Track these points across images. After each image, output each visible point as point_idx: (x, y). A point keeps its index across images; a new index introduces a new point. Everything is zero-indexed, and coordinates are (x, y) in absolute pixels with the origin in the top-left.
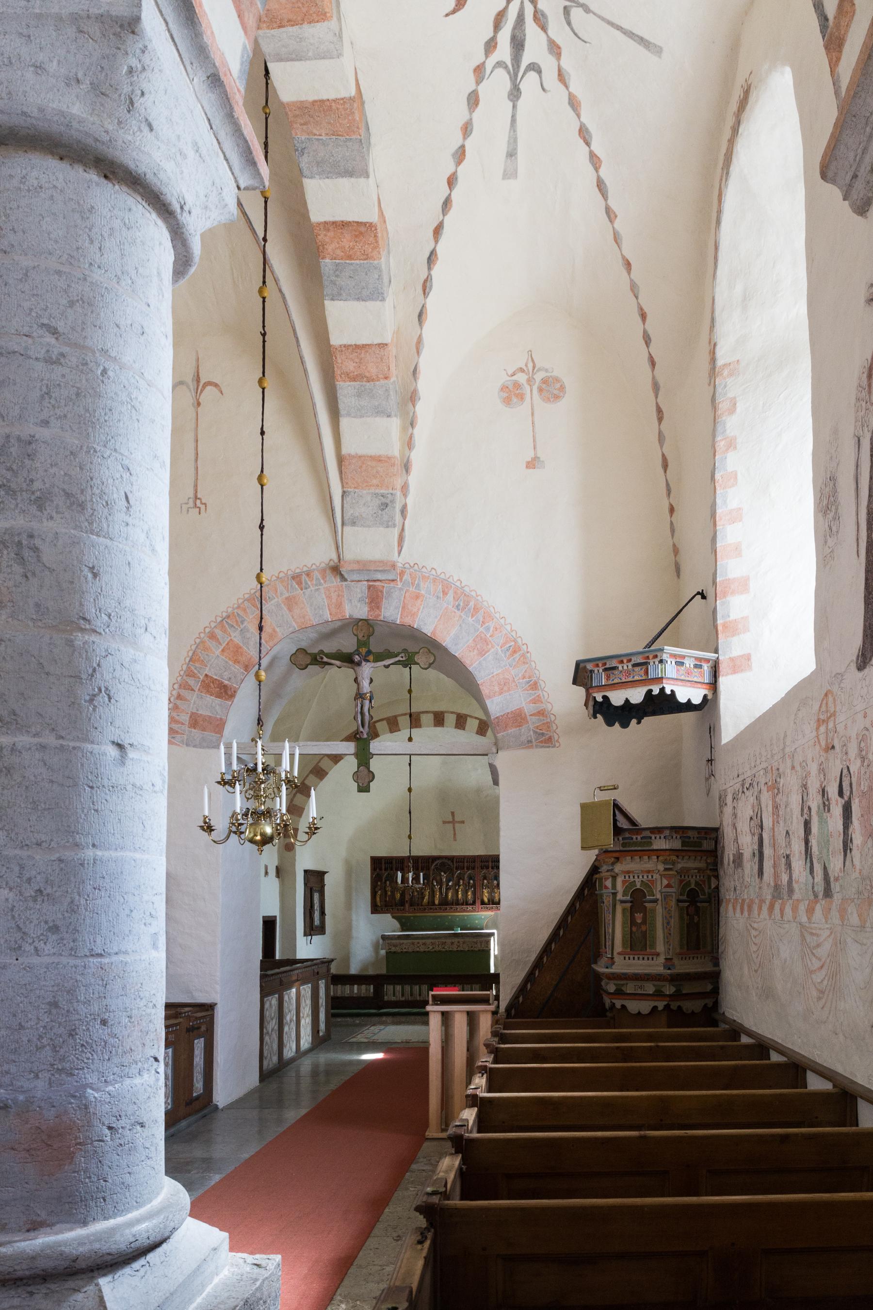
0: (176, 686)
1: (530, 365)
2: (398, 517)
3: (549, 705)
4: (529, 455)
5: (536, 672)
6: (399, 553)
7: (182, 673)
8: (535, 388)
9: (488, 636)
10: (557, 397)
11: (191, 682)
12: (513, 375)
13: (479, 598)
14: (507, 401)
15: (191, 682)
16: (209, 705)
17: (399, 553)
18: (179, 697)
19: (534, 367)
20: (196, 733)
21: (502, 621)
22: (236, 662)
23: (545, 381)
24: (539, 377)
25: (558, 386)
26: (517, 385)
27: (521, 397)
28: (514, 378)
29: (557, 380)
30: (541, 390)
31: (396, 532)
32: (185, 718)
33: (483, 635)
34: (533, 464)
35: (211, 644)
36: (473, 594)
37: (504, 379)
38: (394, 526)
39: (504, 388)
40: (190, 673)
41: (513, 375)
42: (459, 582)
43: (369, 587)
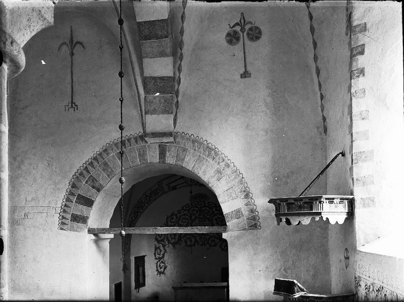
0: (64, 200)
1: (242, 21)
2: (174, 107)
3: (254, 206)
4: (242, 71)
5: (248, 189)
6: (175, 127)
7: (67, 193)
8: (245, 34)
9: (222, 170)
10: (258, 38)
11: (71, 198)
12: (234, 26)
13: (217, 149)
14: (230, 42)
15: (71, 198)
16: (80, 210)
17: (175, 127)
18: (66, 206)
19: (244, 22)
20: (75, 224)
21: (229, 162)
22: (93, 187)
23: (251, 29)
24: (247, 27)
25: (257, 31)
26: (235, 32)
27: (238, 39)
28: (234, 29)
29: (257, 28)
30: (248, 34)
31: (172, 116)
32: (69, 216)
33: (219, 170)
34: (245, 75)
35: (81, 178)
36: (213, 147)
37: (227, 30)
38: (172, 113)
39: (228, 35)
40: (72, 194)
41: (234, 26)
42: (206, 141)
43: (159, 145)
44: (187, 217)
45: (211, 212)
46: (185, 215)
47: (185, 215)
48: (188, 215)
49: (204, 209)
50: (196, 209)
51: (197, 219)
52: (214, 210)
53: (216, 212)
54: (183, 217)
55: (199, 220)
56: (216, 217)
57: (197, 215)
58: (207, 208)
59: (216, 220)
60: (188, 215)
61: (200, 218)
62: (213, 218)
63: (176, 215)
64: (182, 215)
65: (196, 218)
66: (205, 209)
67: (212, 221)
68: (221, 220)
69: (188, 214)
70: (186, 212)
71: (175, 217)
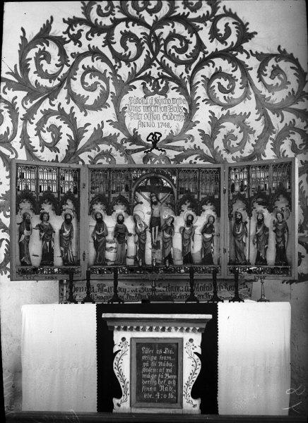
44: (101, 66)
45: (191, 47)
46: (94, 52)
47: (94, 52)
48: (105, 59)
49: (166, 30)
50: (138, 30)
51: (138, 83)
52: (204, 34)
53: (212, 46)
54: (87, 61)
55: (147, 94)
56: (207, 71)
57: (140, 62)
58: (180, 28)
59: (208, 82)
60: (105, 59)
61: (148, 78)
62: (198, 78)
63: (60, 42)
64: (85, 55)
65: (134, 76)
66: (172, 36)
67: (193, 88)
68: (225, 83)
69: (106, 51)
70: (98, 41)
71: (53, 49)
